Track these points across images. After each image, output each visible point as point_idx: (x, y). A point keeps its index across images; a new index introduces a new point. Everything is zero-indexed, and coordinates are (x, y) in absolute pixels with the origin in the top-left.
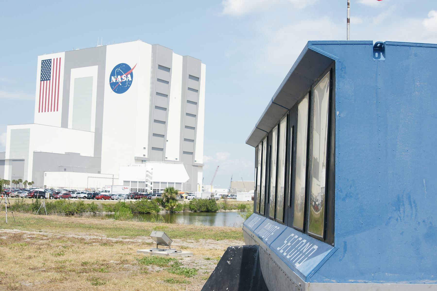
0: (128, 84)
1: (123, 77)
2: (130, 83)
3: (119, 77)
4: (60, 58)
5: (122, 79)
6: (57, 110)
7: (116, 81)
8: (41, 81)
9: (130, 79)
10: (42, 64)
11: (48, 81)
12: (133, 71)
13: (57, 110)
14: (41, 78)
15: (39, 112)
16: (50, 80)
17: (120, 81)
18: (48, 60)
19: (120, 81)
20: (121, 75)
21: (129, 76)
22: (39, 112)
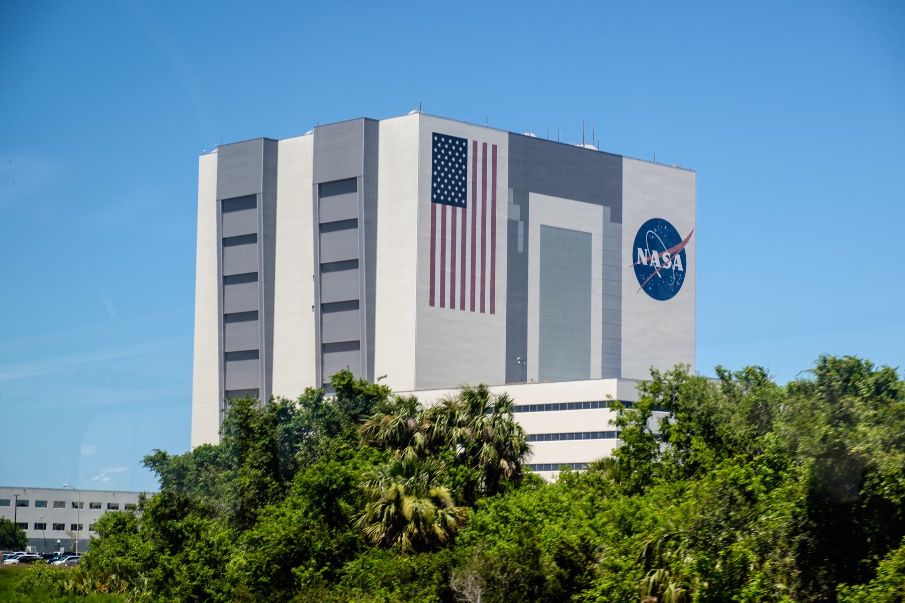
0: (677, 277)
3: (655, 253)
4: (495, 147)
6: (492, 311)
7: (649, 262)
8: (434, 201)
9: (681, 269)
10: (435, 144)
11: (459, 210)
12: (686, 247)
13: (492, 311)
14: (434, 190)
15: (432, 303)
16: (464, 206)
18: (454, 139)
19: (658, 265)
21: (678, 257)
22: (432, 303)
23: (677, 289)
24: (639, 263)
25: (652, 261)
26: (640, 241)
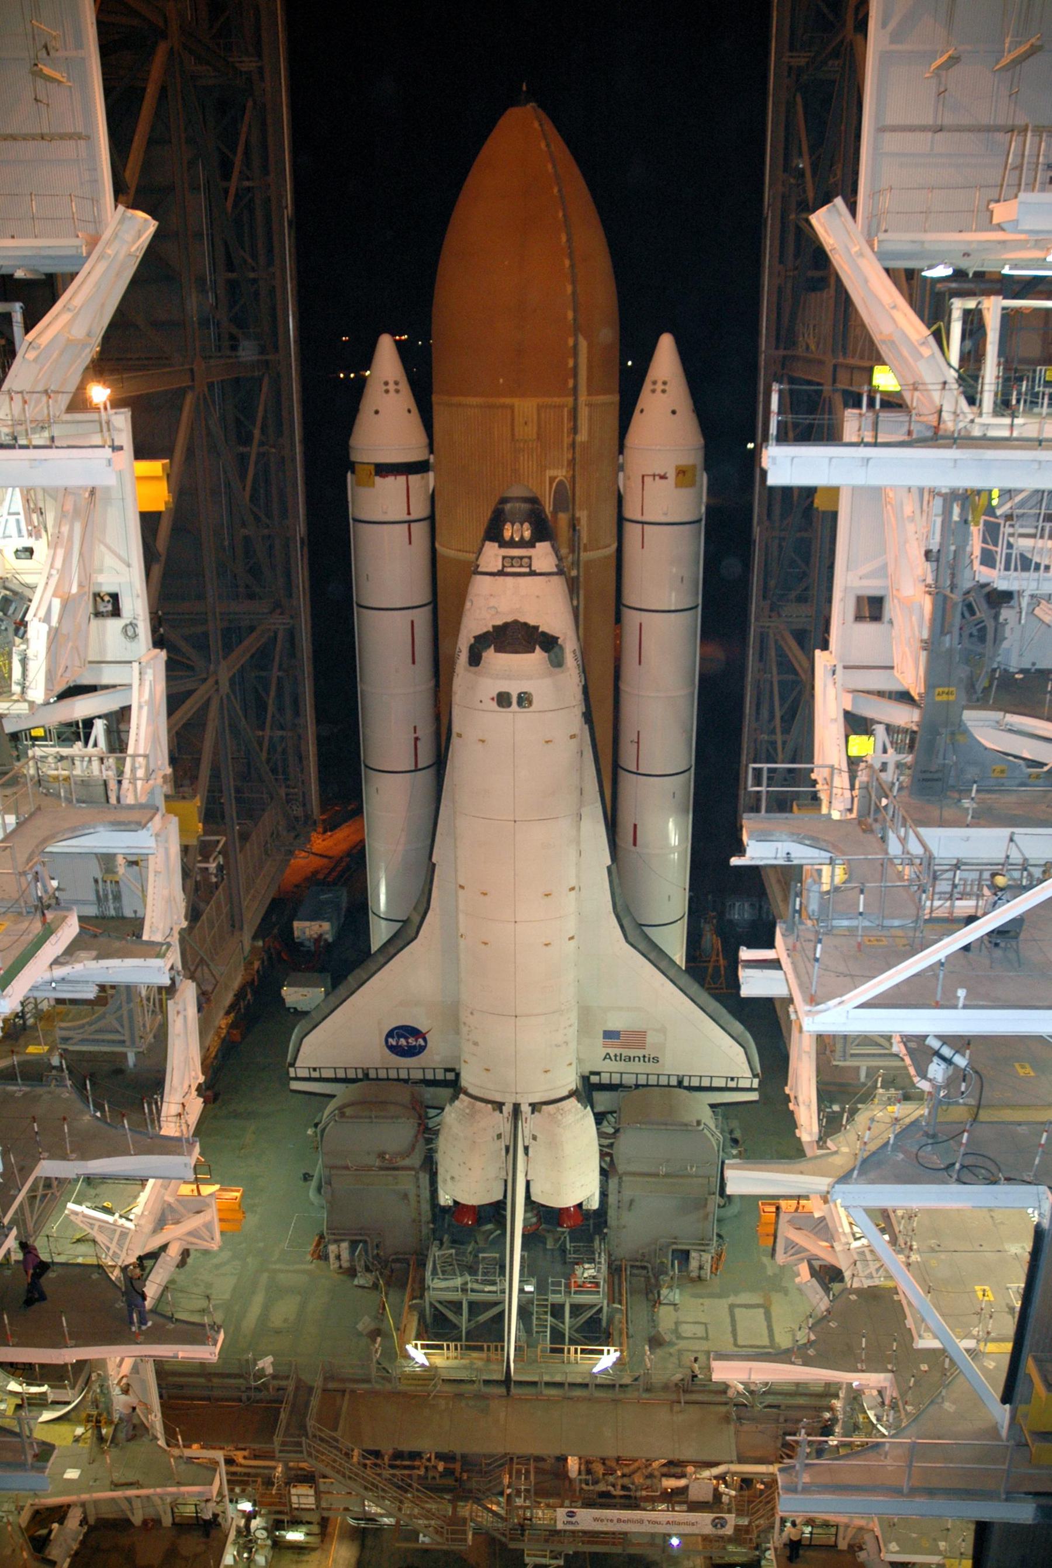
1: (410, 1041)
2: (422, 1049)
9: (423, 1043)
20: (406, 1038)
23: (419, 1053)
26: (390, 1034)
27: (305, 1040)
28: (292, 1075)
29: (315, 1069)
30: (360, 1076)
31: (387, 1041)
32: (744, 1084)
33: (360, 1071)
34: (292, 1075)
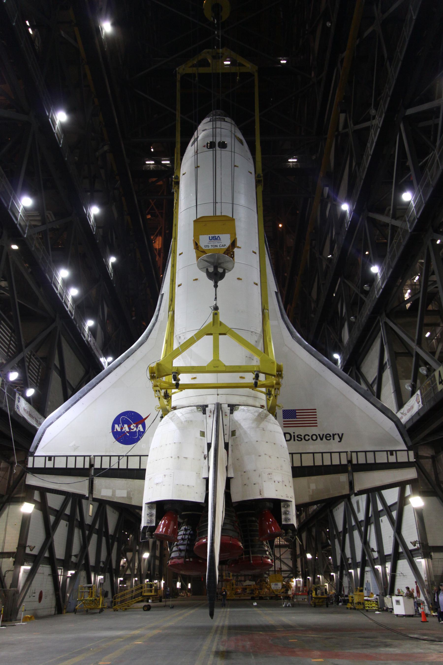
1: (132, 427)
2: (141, 434)
3: (126, 426)
5: (130, 428)
7: (122, 429)
9: (142, 430)
12: (146, 421)
17: (128, 430)
19: (128, 430)
21: (140, 426)
23: (138, 439)
24: (115, 430)
25: (124, 429)
26: (116, 421)
27: (48, 429)
28: (30, 465)
29: (50, 459)
30: (87, 466)
31: (113, 427)
32: (402, 458)
33: (87, 459)
34: (30, 465)
